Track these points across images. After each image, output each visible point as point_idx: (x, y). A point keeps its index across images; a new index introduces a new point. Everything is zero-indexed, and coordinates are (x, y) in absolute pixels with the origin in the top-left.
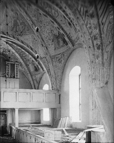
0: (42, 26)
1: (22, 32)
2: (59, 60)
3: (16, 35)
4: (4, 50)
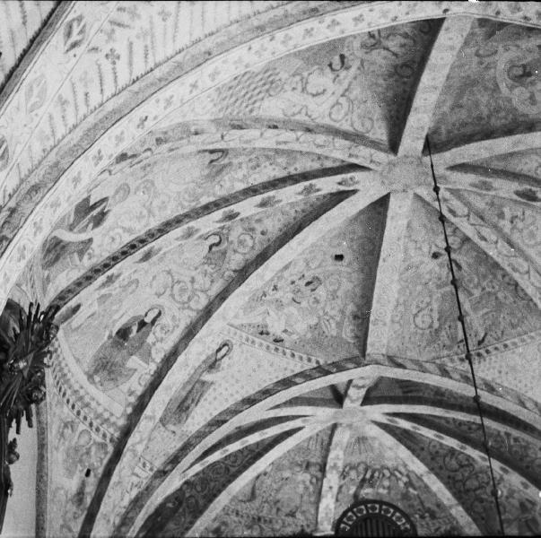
1: (483, 340)
3: (456, 358)
4: (368, 476)
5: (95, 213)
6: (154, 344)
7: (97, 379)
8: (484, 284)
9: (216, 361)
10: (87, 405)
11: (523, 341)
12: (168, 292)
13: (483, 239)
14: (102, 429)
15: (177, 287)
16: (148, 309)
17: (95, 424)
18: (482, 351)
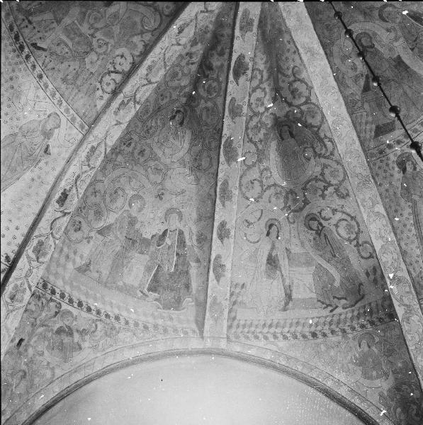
0: (133, 145)
1: (39, 48)
2: (60, 331)
8: (98, 35)
11: (53, 95)
13: (181, 31)
18: (26, 50)
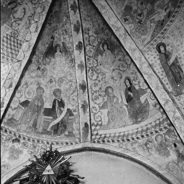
5: (57, 105)
6: (140, 86)
7: (140, 119)
9: (165, 54)
10: (147, 129)
12: (121, 72)
14: (162, 127)
15: (121, 68)
16: (125, 84)
17: (157, 130)
